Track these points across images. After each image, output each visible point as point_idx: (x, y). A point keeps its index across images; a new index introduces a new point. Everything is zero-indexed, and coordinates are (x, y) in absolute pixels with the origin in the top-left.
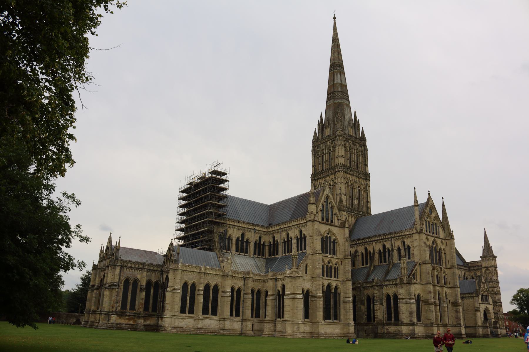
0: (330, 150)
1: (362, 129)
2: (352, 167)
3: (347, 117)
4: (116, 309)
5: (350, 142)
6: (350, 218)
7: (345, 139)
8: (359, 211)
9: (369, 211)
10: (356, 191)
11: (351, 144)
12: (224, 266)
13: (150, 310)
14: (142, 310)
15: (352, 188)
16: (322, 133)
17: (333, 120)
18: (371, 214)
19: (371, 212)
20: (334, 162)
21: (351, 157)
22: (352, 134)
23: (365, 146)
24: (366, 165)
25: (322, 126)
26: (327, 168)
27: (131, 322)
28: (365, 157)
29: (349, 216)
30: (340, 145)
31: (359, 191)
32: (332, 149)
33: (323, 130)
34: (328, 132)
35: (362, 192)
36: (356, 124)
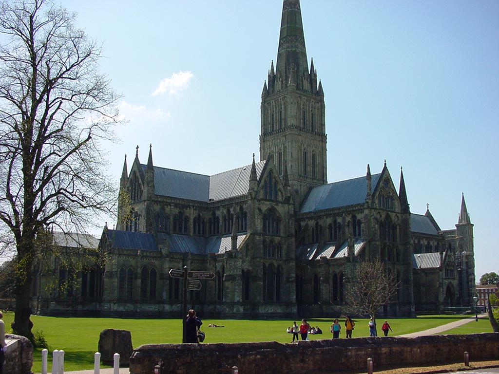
0: (281, 108)
1: (320, 82)
2: (306, 128)
3: (301, 69)
4: (55, 296)
5: (304, 99)
6: (302, 187)
7: (298, 95)
8: (313, 179)
9: (325, 178)
10: (309, 156)
11: (305, 100)
12: (161, 249)
13: (88, 295)
14: (79, 296)
15: (305, 153)
16: (273, 87)
17: (286, 71)
18: (327, 182)
19: (326, 179)
20: (286, 122)
21: (305, 116)
22: (307, 88)
23: (322, 102)
24: (323, 125)
25: (272, 78)
26: (277, 129)
27: (70, 308)
28: (322, 115)
29: (301, 185)
30: (292, 103)
31: (314, 157)
32: (283, 107)
33: (274, 81)
34: (278, 85)
35: (317, 156)
36: (313, 75)
